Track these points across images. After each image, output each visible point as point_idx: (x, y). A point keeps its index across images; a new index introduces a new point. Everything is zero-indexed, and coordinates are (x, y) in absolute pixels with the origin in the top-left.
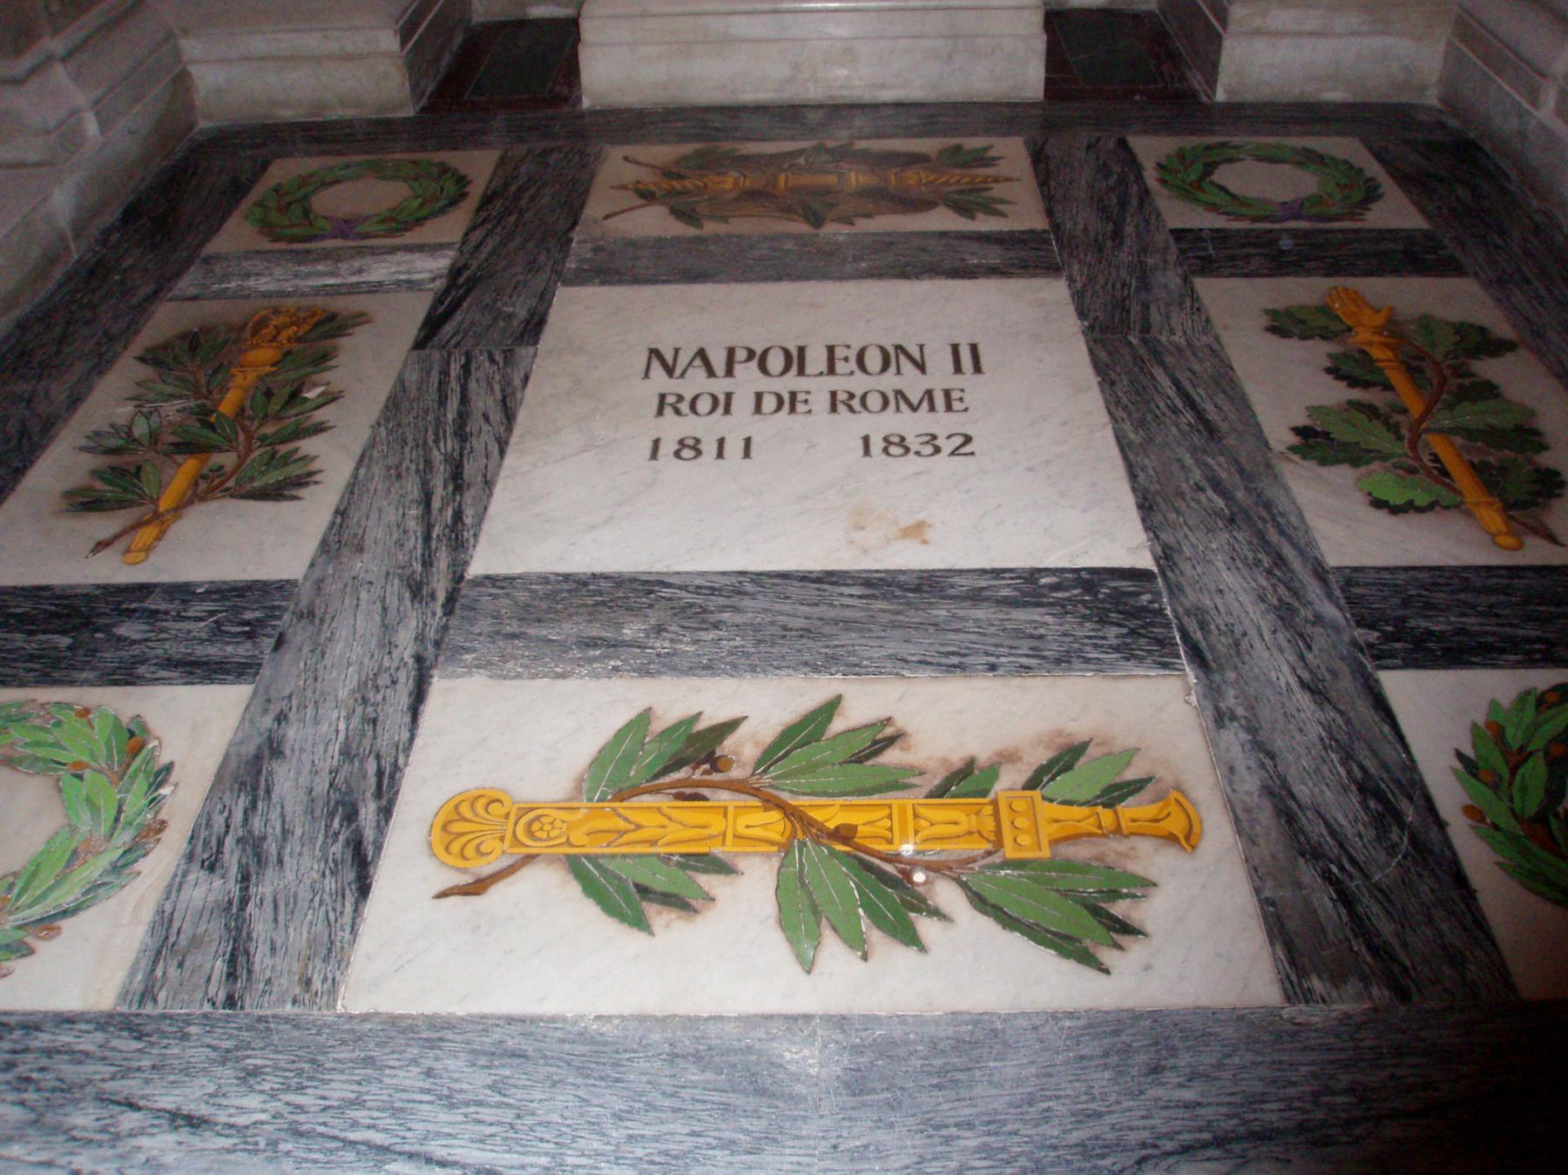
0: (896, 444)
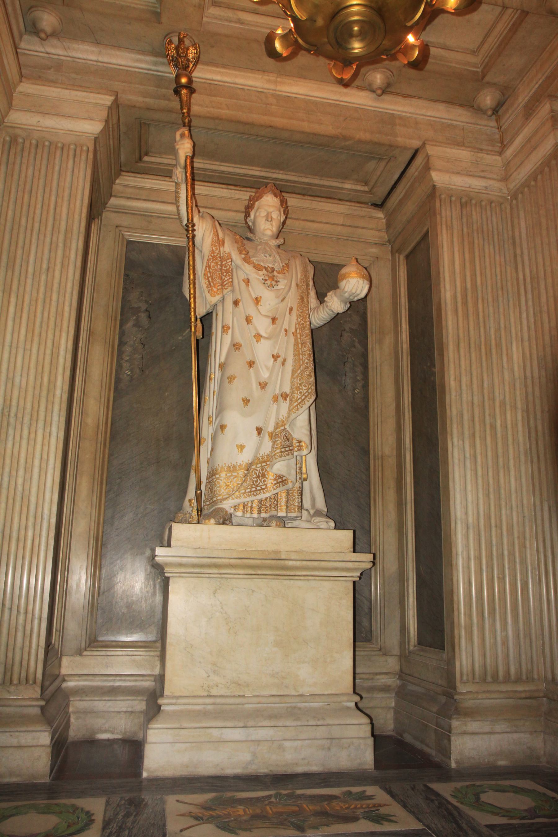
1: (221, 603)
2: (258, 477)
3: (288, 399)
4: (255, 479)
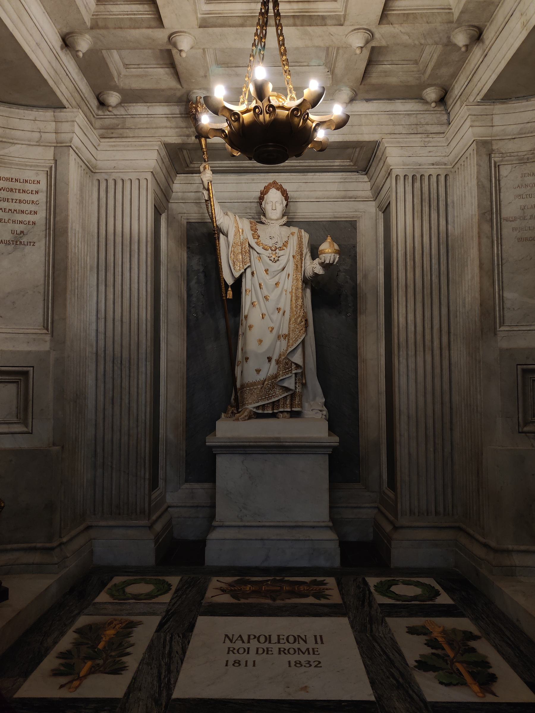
0: (298, 664)
1: (247, 468)
2: (270, 389)
3: (287, 338)
4: (268, 390)
